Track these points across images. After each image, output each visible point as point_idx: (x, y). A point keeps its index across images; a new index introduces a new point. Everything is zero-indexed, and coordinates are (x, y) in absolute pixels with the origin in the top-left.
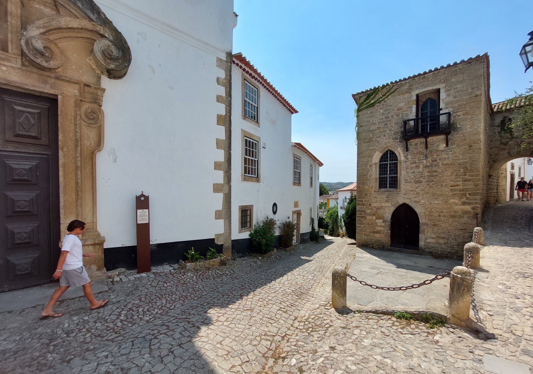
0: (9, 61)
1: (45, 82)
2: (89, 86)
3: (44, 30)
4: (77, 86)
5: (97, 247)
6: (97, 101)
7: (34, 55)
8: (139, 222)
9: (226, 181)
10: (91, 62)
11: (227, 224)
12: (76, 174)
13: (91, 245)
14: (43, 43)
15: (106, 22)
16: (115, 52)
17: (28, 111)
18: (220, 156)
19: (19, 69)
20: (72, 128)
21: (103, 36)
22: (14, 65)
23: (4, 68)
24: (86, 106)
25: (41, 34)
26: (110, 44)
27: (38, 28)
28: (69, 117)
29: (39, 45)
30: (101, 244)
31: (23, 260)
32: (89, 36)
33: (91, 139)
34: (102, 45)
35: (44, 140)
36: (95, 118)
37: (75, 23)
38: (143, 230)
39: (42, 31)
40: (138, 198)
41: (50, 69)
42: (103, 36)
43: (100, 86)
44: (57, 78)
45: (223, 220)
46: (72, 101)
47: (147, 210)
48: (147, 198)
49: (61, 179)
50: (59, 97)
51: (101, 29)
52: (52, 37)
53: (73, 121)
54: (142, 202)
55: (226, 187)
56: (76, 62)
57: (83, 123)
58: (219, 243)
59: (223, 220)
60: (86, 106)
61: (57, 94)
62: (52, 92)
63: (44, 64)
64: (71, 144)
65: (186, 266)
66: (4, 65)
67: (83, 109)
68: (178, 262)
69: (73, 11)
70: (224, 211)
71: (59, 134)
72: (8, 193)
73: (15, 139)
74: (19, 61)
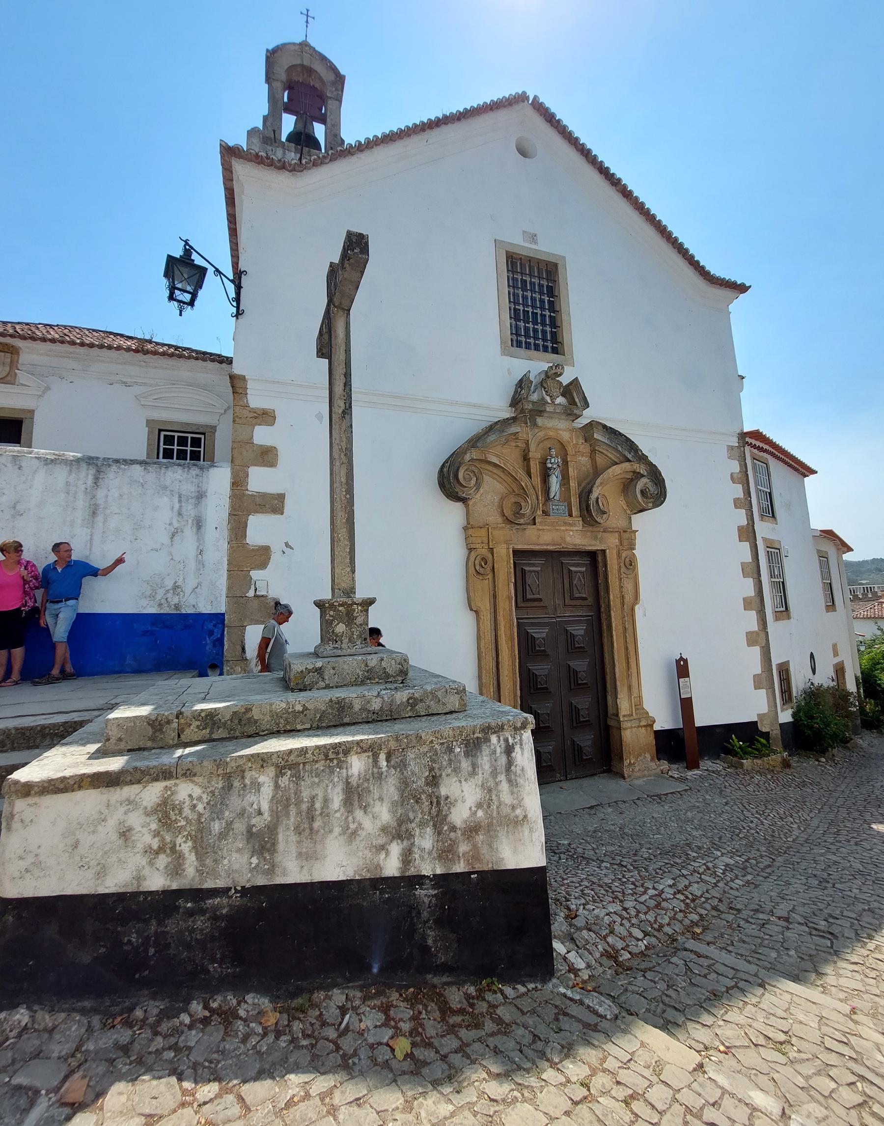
1: (596, 538)
5: (649, 728)
6: (632, 547)
8: (683, 697)
9: (761, 626)
11: (771, 699)
12: (625, 637)
13: (644, 726)
15: (642, 458)
16: (652, 488)
17: (579, 569)
18: (748, 588)
30: (651, 726)
31: (586, 740)
35: (590, 601)
38: (687, 706)
40: (678, 662)
44: (604, 531)
45: (764, 691)
47: (687, 679)
48: (686, 661)
49: (615, 644)
54: (682, 669)
55: (762, 635)
58: (764, 730)
59: (764, 691)
64: (618, 601)
65: (742, 765)
68: (718, 758)
69: (609, 455)
70: (764, 675)
72: (571, 663)
73: (572, 603)
74: (581, 522)
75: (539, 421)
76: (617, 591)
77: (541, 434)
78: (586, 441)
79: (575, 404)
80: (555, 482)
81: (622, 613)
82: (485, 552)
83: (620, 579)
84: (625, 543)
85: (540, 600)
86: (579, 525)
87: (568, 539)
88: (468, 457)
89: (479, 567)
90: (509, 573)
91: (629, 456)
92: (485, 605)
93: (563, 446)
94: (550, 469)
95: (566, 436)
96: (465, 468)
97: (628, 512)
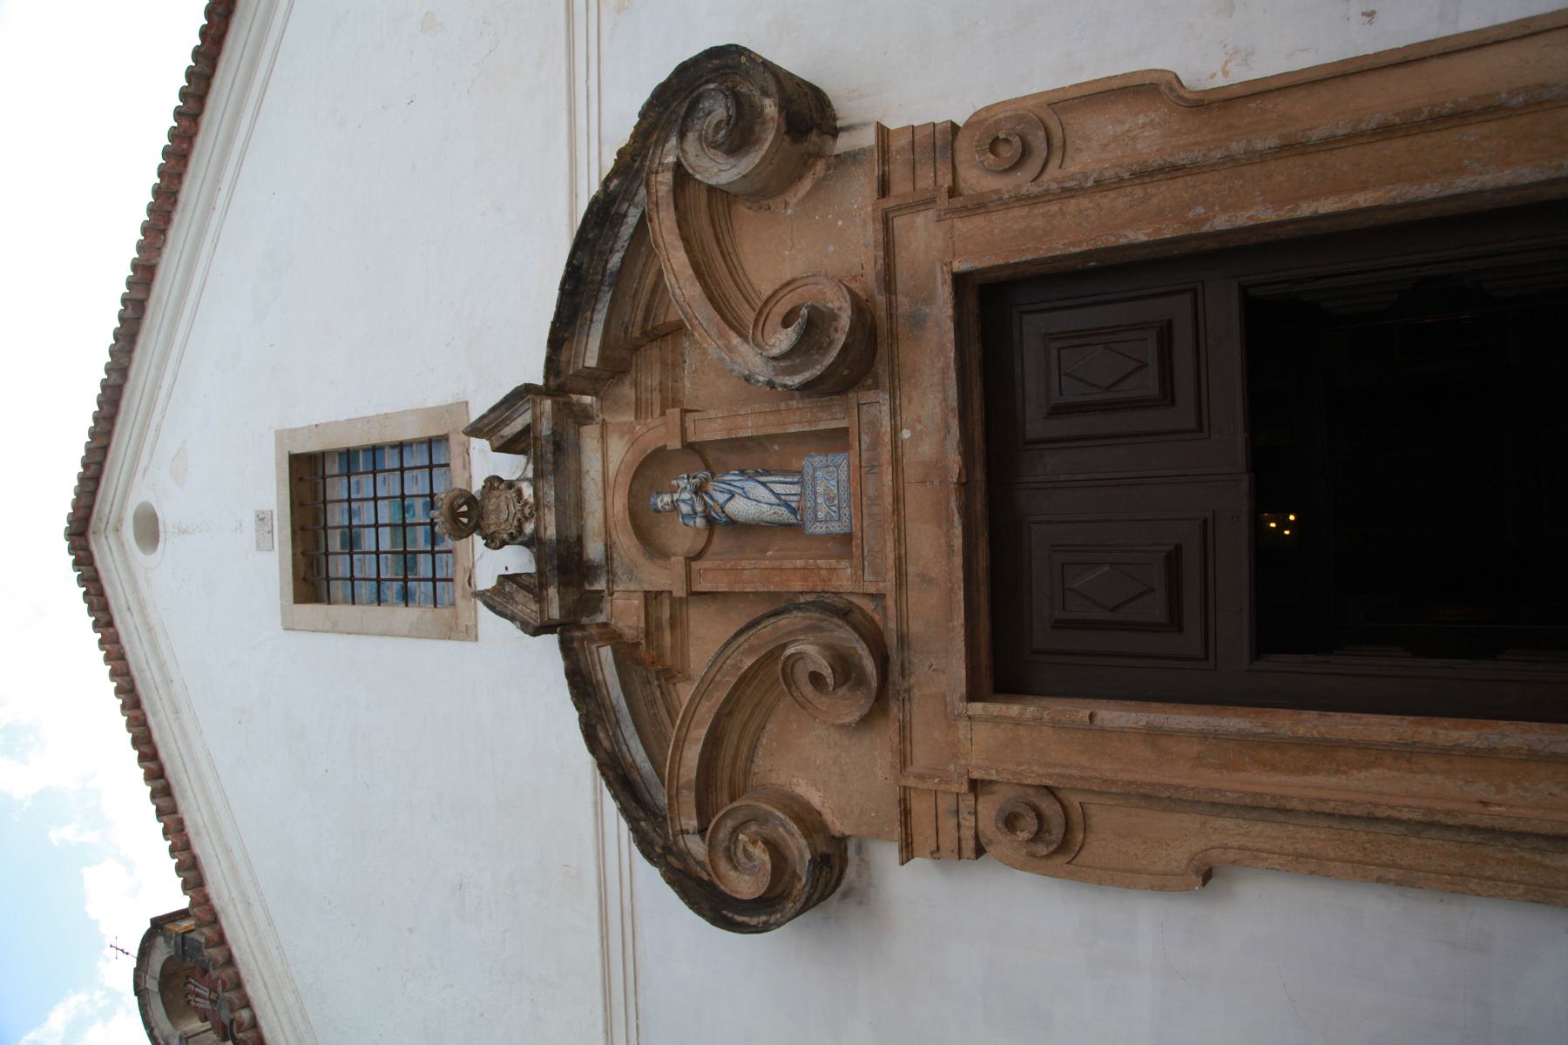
0: (875, 424)
1: (918, 322)
2: (884, 188)
3: (733, 334)
4: (899, 223)
6: (944, 141)
7: (823, 349)
10: (793, 200)
12: (1330, 143)
14: (775, 332)
15: (631, 165)
16: (717, 110)
19: (893, 397)
20: (1085, 202)
21: (681, 175)
22: (886, 408)
23: (906, 434)
24: (976, 178)
25: (743, 337)
26: (691, 137)
27: (730, 349)
28: (1039, 222)
29: (783, 340)
32: (704, 221)
33: (1120, 129)
34: (706, 163)
36: (1019, 137)
37: (676, 259)
39: (735, 340)
41: (861, 308)
42: (681, 175)
43: (871, 150)
46: (963, 226)
50: (959, 266)
51: (664, 181)
52: (749, 316)
53: (1054, 208)
56: (809, 250)
57: (1053, 171)
60: (976, 178)
61: (949, 278)
62: (944, 293)
63: (845, 321)
66: (895, 432)
67: (989, 183)
71: (1123, 241)
75: (594, 550)
76: (1118, 201)
77: (626, 542)
78: (625, 372)
79: (527, 429)
80: (751, 500)
81: (1214, 167)
82: (988, 809)
83: (1067, 193)
84: (925, 181)
85: (1174, 560)
86: (878, 406)
87: (927, 449)
88: (697, 847)
89: (1048, 832)
90: (1057, 725)
91: (632, 218)
92: (1185, 836)
93: (650, 469)
94: (711, 522)
95: (618, 449)
96: (724, 866)
97: (820, 166)
